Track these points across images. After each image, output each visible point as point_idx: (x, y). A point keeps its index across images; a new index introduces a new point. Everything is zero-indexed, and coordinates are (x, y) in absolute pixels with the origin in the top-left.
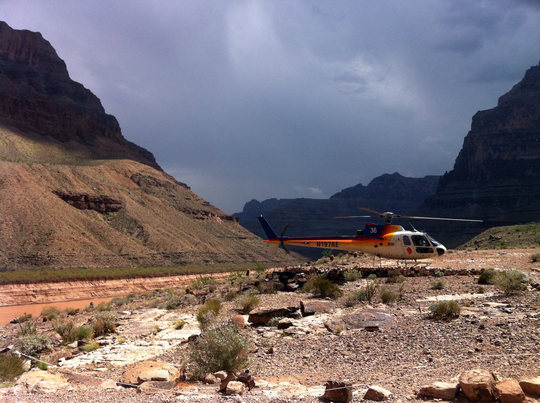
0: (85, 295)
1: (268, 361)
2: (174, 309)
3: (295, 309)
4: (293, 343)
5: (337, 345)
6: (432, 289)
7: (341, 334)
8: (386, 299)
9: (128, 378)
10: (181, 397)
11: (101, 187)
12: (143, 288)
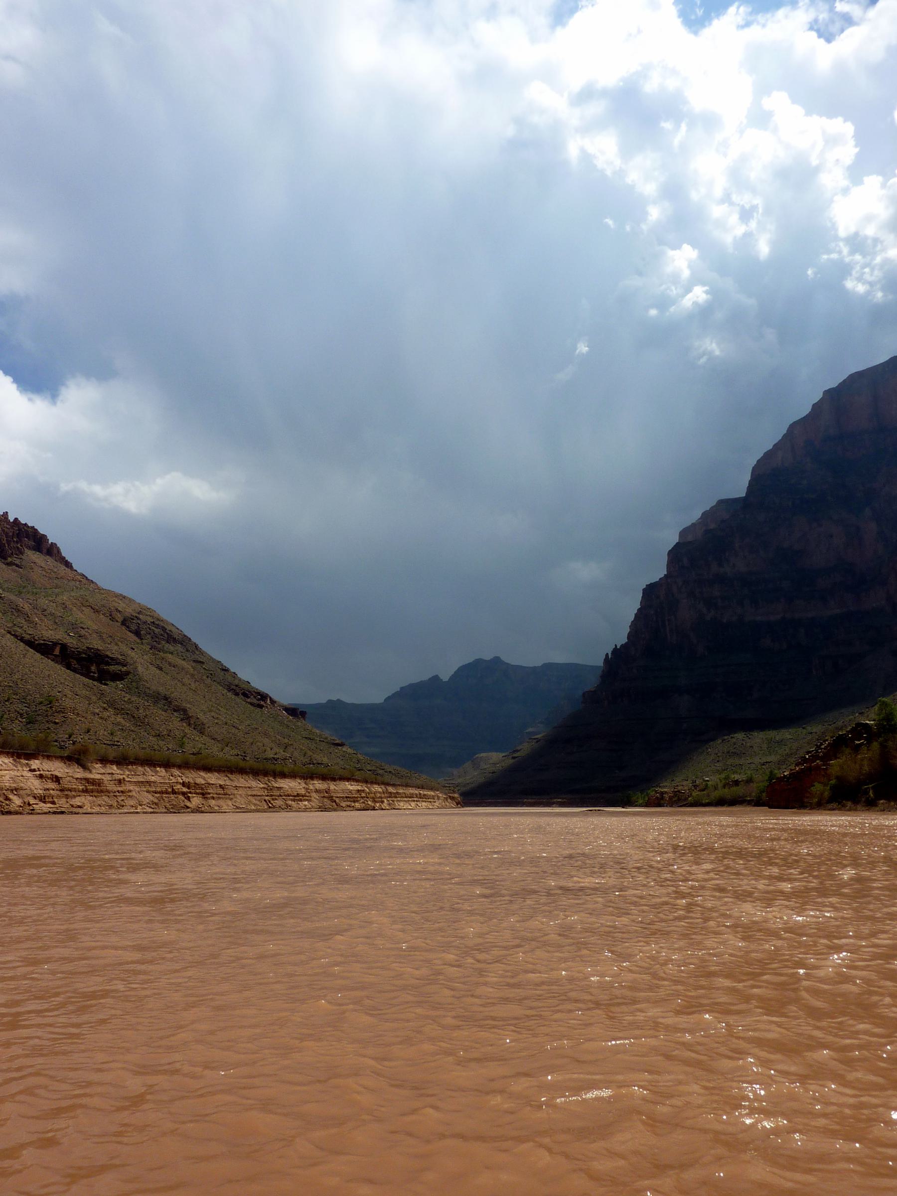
11: (83, 632)
12: (331, 799)
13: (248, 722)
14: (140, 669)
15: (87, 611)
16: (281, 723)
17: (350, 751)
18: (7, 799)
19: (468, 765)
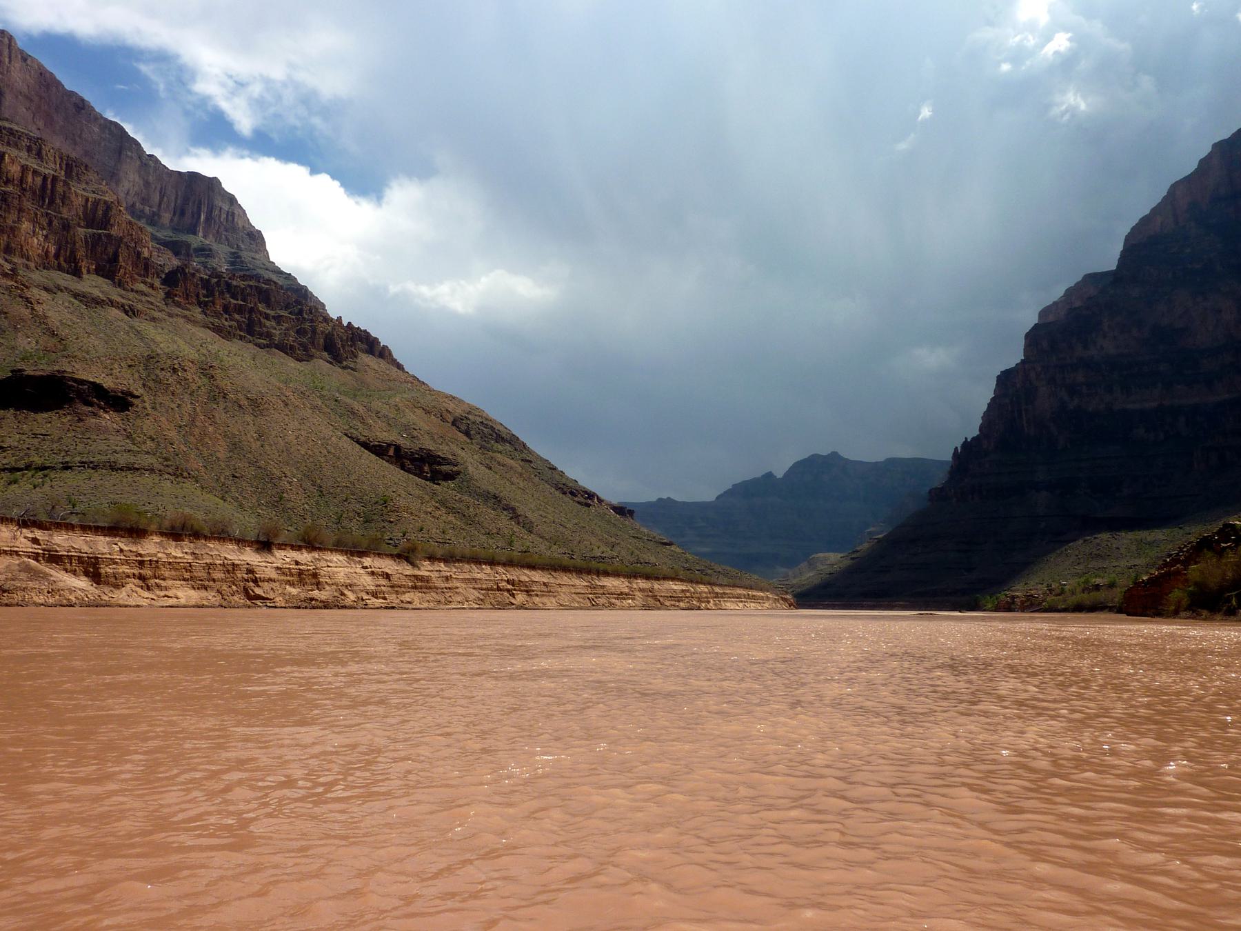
11: (415, 433)
12: (655, 597)
13: (576, 521)
15: (419, 412)
16: (609, 522)
17: (678, 550)
18: (343, 594)
19: (804, 565)
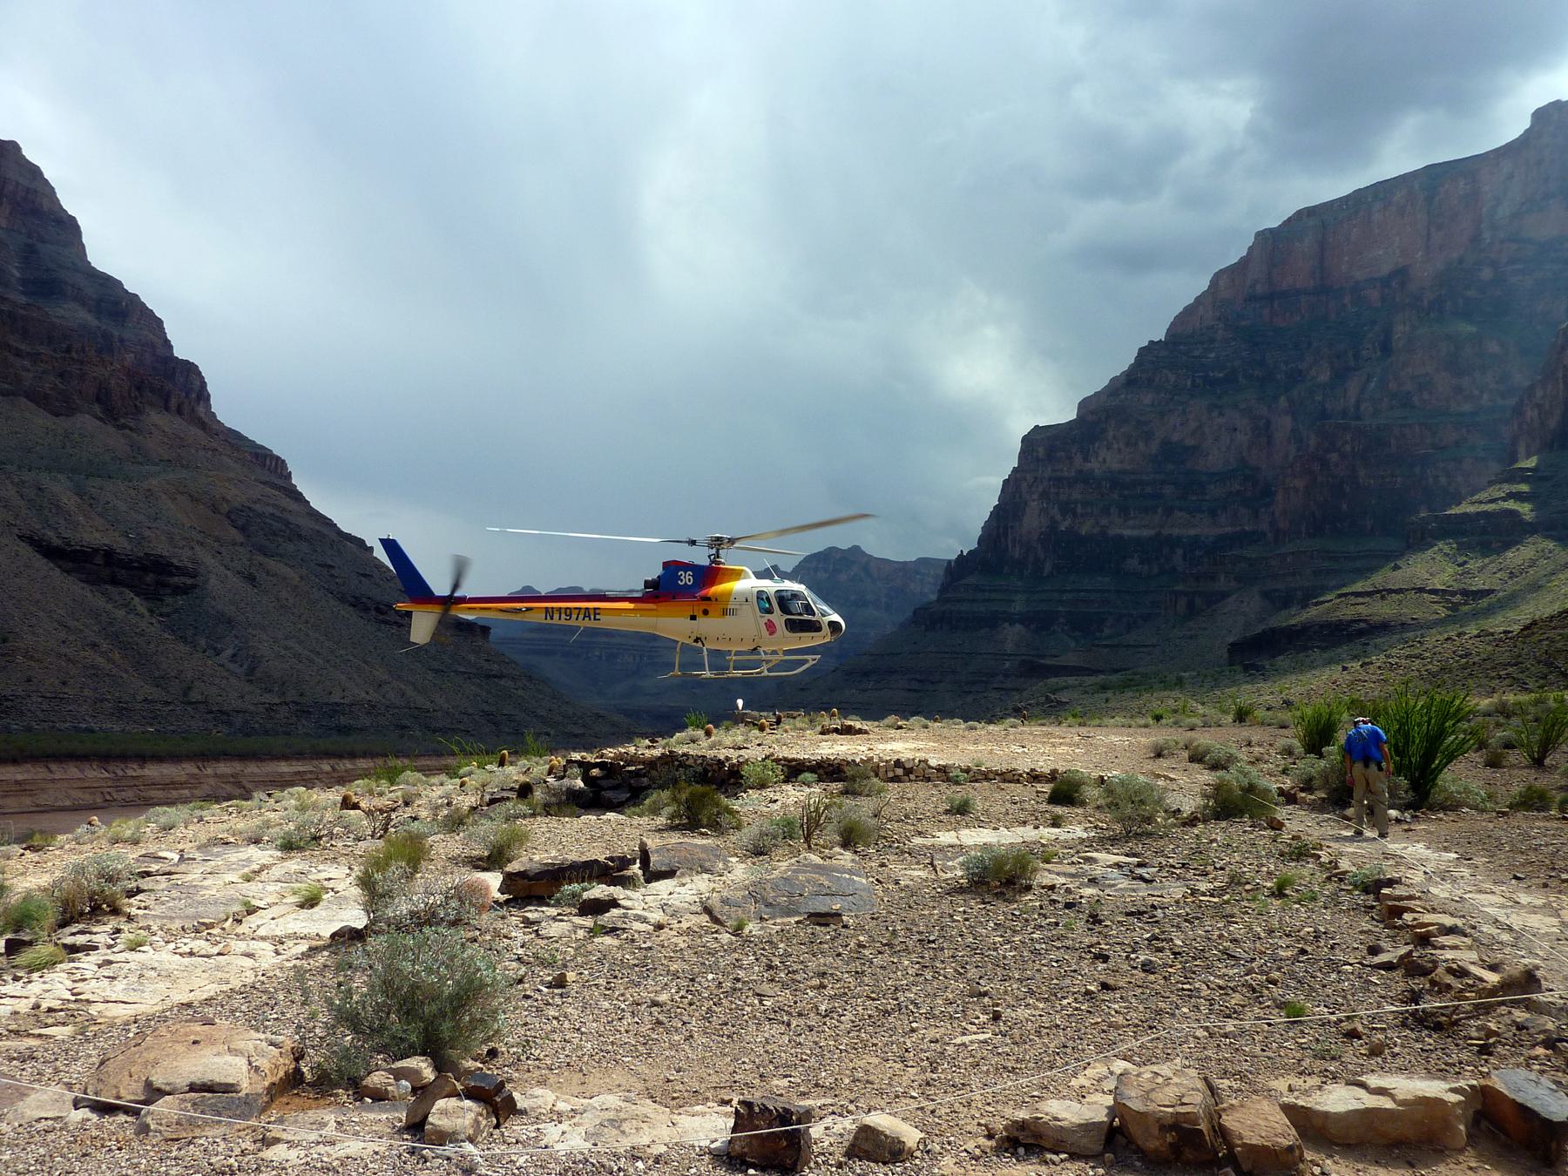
0: (87, 798)
1: (552, 1012)
2: (300, 849)
3: (624, 862)
4: (619, 956)
5: (737, 964)
6: (947, 812)
7: (746, 931)
8: (850, 838)
9: (113, 1081)
10: (276, 1153)
11: (147, 533)
12: (239, 785)
14: (213, 581)
